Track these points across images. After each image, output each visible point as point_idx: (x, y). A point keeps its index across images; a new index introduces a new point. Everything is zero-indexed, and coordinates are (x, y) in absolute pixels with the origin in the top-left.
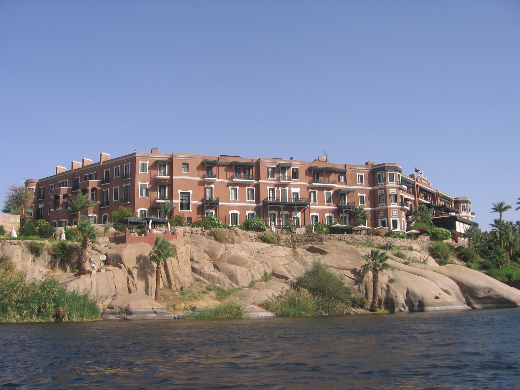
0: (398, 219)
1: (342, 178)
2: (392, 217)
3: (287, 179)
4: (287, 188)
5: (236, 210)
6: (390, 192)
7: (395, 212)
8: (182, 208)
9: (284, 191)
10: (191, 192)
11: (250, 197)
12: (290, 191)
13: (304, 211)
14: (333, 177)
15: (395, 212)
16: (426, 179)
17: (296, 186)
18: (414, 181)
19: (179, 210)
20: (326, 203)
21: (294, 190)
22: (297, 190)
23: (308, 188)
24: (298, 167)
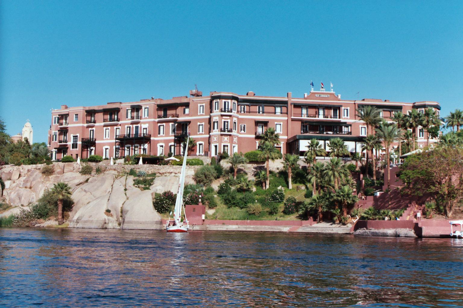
0: (217, 144)
1: (187, 111)
2: (213, 143)
3: (135, 118)
4: (139, 125)
5: (107, 145)
6: (214, 119)
7: (215, 138)
8: (73, 148)
9: (137, 128)
10: (78, 135)
11: (107, 135)
12: (141, 127)
13: (150, 143)
14: (180, 110)
15: (215, 138)
16: (332, 92)
17: (145, 123)
18: (286, 99)
19: (71, 149)
20: (171, 134)
21: (144, 126)
22: (146, 126)
23: (159, 122)
24: (148, 107)
